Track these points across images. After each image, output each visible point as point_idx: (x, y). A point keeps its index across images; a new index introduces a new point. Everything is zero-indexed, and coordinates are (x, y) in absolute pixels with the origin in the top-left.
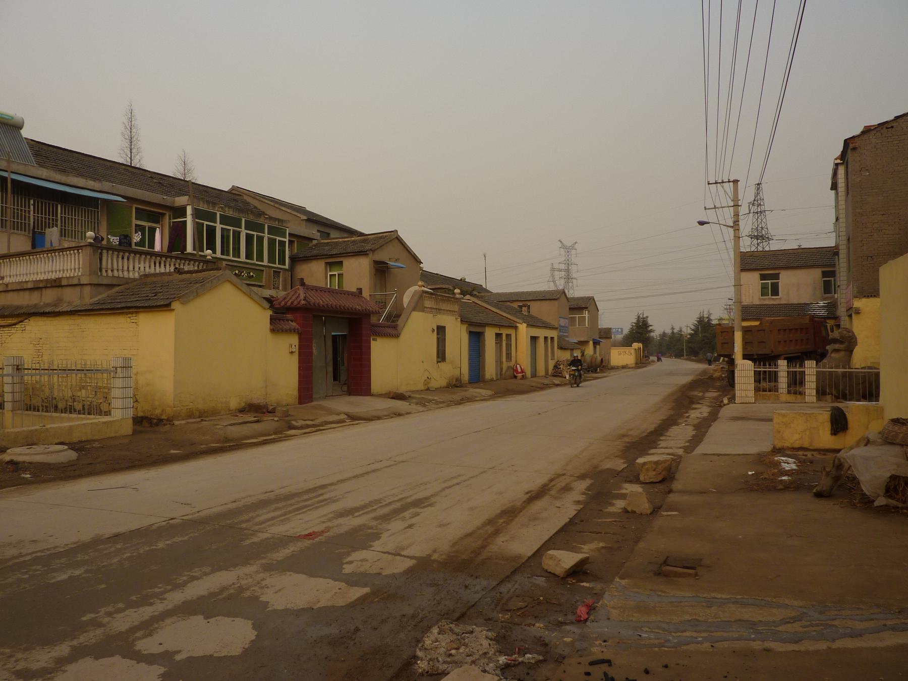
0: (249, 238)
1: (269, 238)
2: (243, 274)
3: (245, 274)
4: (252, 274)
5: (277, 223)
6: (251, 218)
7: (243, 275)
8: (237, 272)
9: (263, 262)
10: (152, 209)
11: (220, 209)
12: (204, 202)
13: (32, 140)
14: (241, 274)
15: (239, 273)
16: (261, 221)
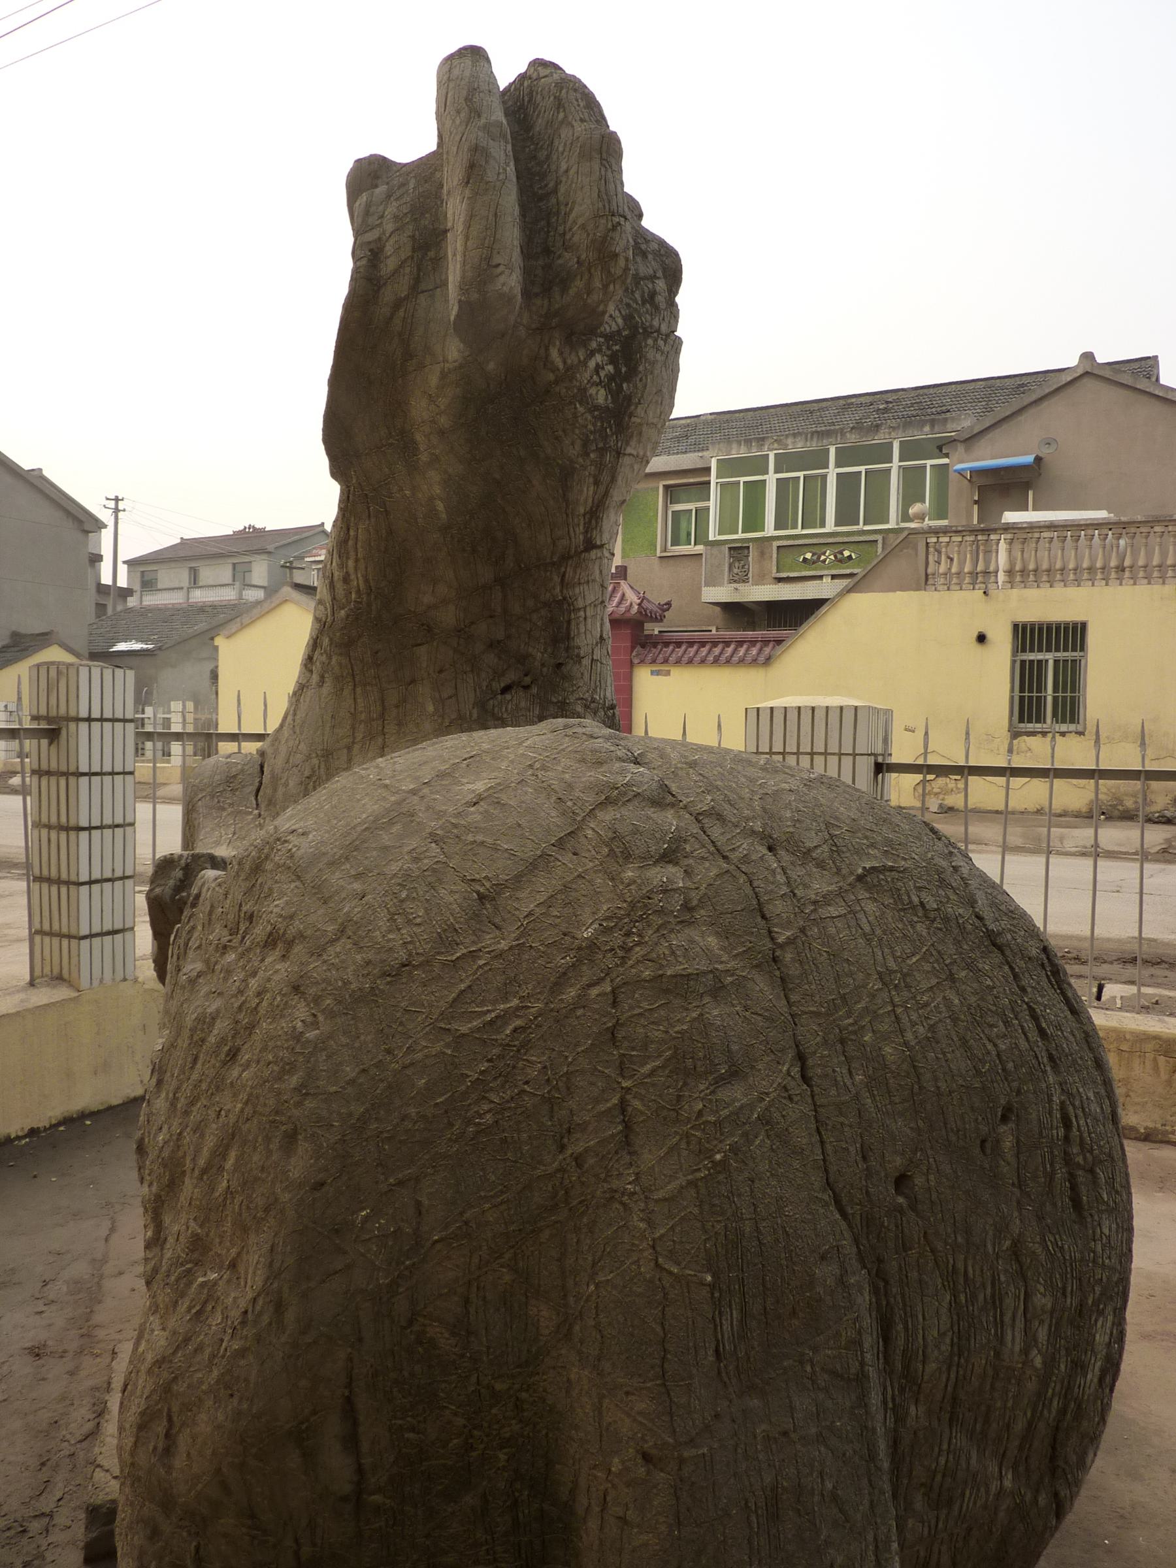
0: (847, 484)
1: (904, 469)
2: (823, 558)
3: (829, 556)
4: (846, 553)
5: (927, 429)
6: (852, 438)
7: (824, 561)
8: (808, 556)
9: (887, 522)
10: (692, 480)
11: (776, 445)
12: (739, 443)
13: (711, 414)
14: (819, 557)
15: (815, 558)
16: (878, 439)
